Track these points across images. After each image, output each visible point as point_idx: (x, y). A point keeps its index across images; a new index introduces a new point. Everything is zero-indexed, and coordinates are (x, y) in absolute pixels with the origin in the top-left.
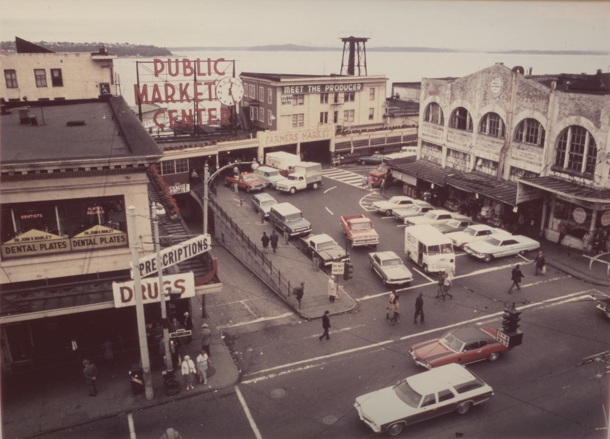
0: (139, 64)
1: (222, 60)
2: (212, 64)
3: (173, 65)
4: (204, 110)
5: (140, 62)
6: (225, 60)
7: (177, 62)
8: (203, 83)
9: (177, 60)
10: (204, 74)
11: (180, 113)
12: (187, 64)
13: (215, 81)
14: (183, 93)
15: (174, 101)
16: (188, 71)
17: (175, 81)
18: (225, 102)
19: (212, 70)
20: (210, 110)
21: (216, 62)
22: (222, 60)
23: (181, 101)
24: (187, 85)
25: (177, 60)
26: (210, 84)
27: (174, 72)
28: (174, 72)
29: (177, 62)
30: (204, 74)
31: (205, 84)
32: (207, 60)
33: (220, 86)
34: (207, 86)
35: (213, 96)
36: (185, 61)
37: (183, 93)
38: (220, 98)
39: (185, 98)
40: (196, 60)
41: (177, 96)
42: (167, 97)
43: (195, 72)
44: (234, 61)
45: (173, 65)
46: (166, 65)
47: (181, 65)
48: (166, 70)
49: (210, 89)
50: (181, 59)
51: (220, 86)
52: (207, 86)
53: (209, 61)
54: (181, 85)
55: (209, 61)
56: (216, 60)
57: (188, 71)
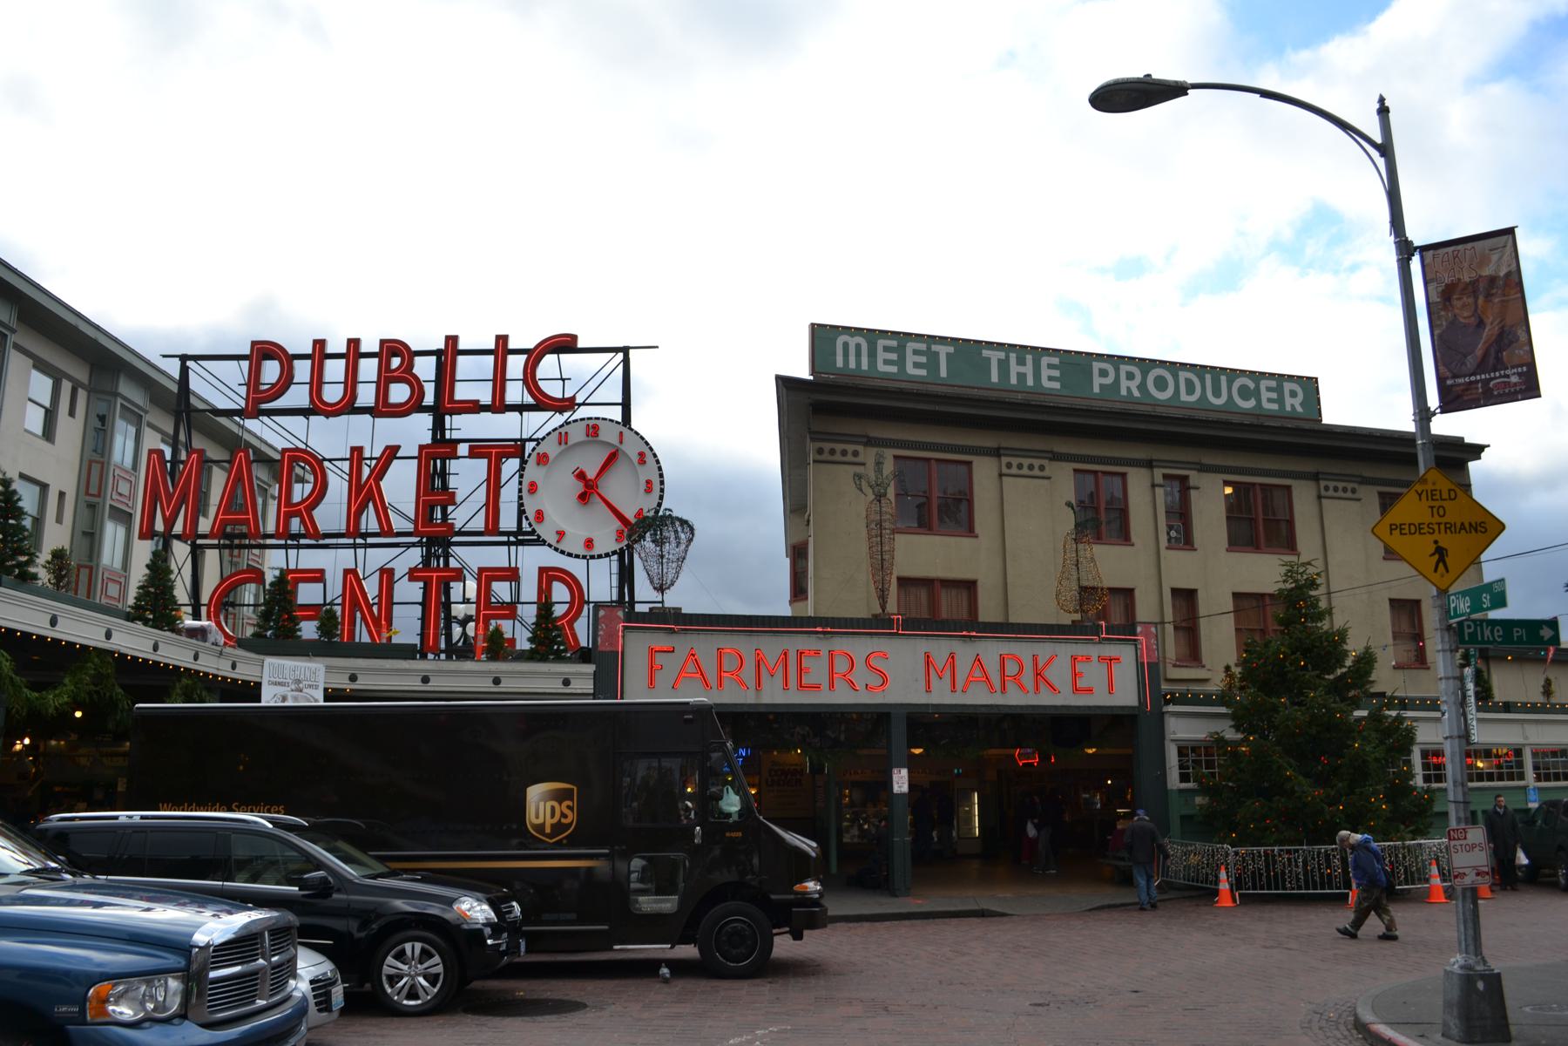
0: (189, 363)
1: (564, 344)
2: (515, 365)
3: (335, 370)
4: (459, 575)
5: (196, 358)
6: (580, 345)
7: (354, 350)
8: (463, 449)
9: (354, 343)
10: (474, 407)
11: (335, 587)
12: (396, 362)
13: (524, 441)
14: (365, 493)
15: (317, 538)
16: (399, 393)
17: (329, 438)
18: (561, 534)
19: (515, 393)
20: (487, 576)
21: (534, 356)
22: (564, 344)
23: (354, 533)
24: (391, 453)
25: (354, 343)
26: (492, 452)
27: (333, 394)
28: (333, 394)
29: (354, 350)
30: (474, 407)
31: (474, 453)
32: (492, 346)
33: (543, 459)
34: (485, 462)
35: (508, 521)
36: (391, 348)
37: (365, 493)
38: (540, 516)
39: (370, 521)
40: (442, 346)
41: (332, 513)
42: (289, 510)
43: (445, 406)
44: (625, 350)
45: (335, 370)
46: (302, 370)
47: (369, 369)
48: (298, 396)
49: (494, 484)
50: (370, 344)
51: (543, 459)
52: (485, 462)
53: (502, 348)
54: (357, 452)
55: (502, 348)
56: (531, 346)
57: (399, 393)
